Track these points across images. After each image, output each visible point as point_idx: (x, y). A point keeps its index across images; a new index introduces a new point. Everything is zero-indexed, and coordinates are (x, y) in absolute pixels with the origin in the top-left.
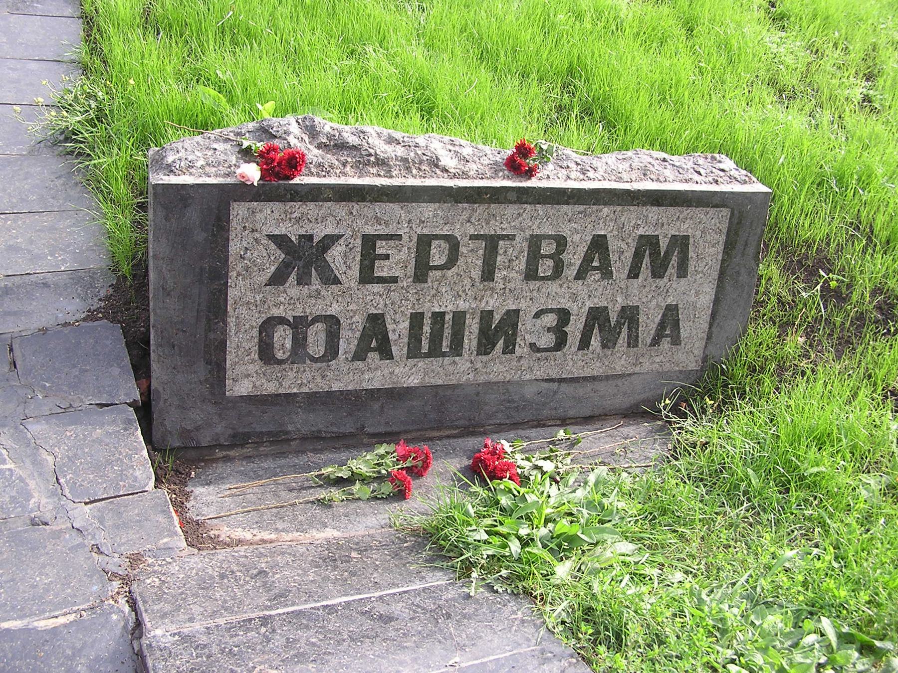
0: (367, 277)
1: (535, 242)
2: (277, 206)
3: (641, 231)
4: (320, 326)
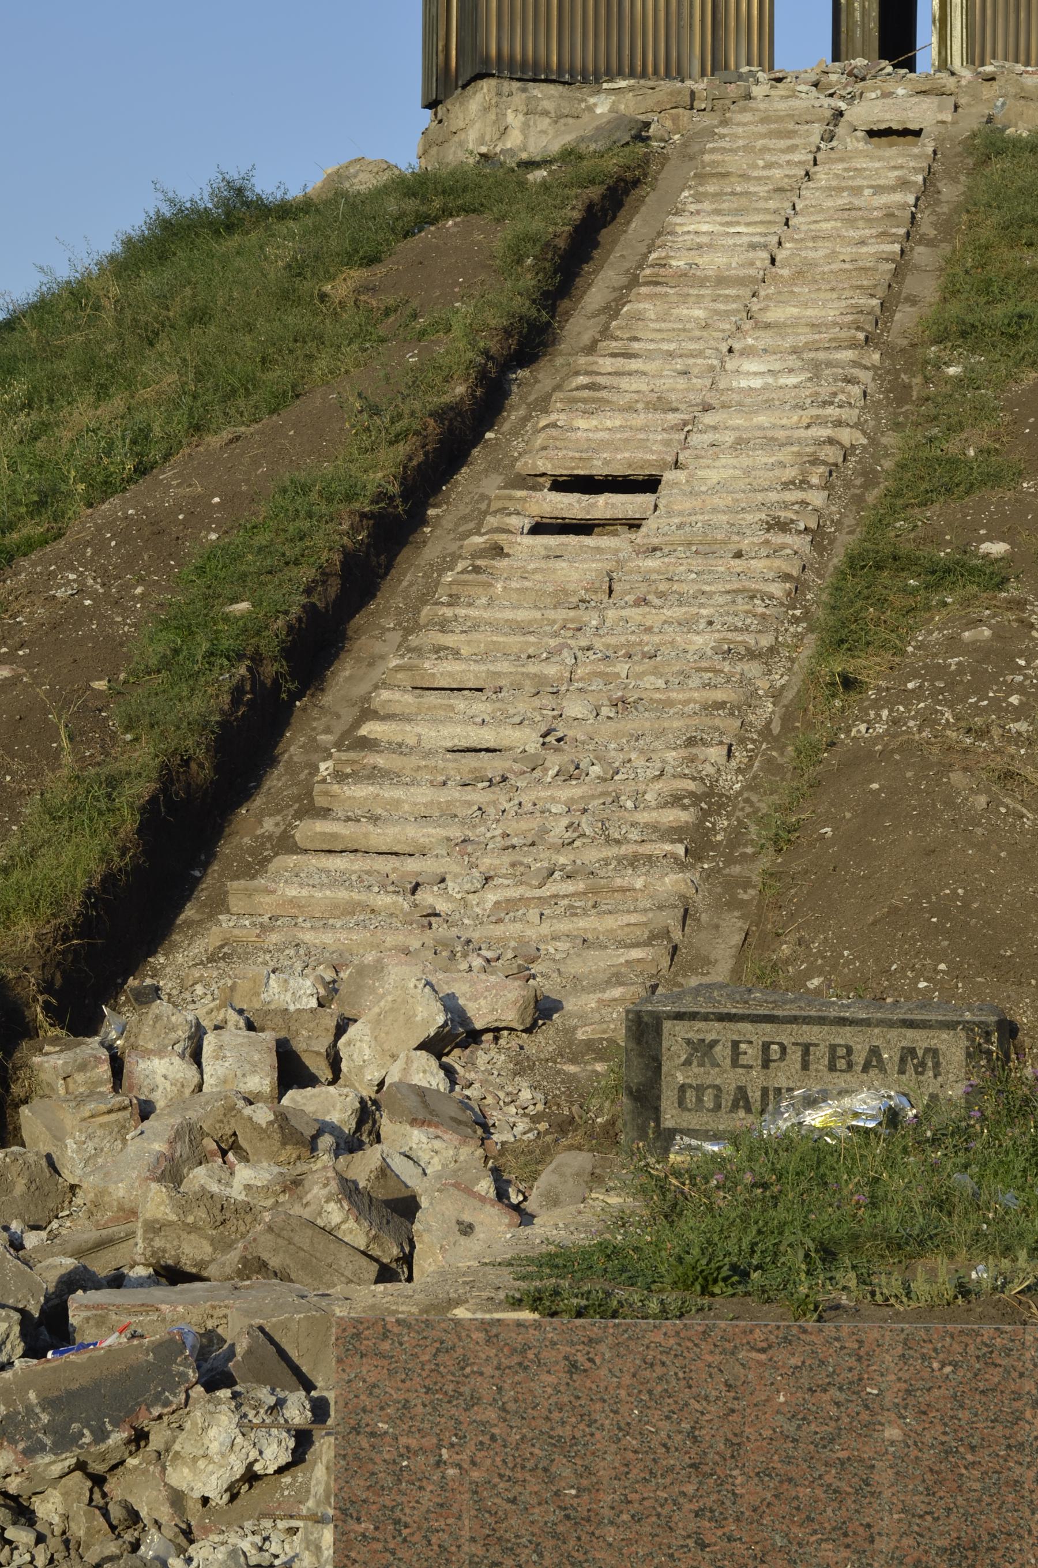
0: (735, 1063)
1: (833, 1048)
2: (686, 1023)
3: (903, 1044)
4: (710, 1090)
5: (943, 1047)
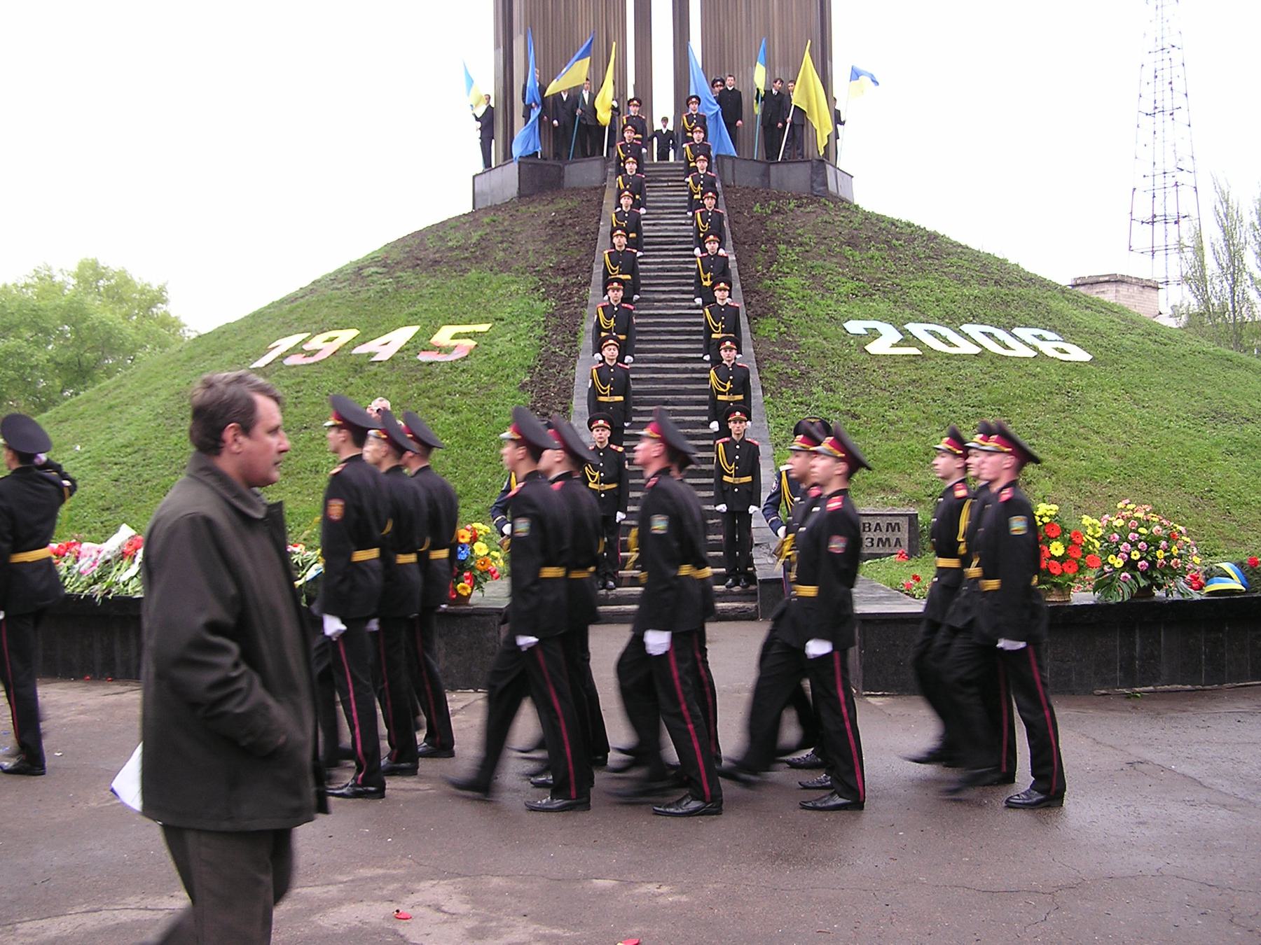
5: (901, 522)
